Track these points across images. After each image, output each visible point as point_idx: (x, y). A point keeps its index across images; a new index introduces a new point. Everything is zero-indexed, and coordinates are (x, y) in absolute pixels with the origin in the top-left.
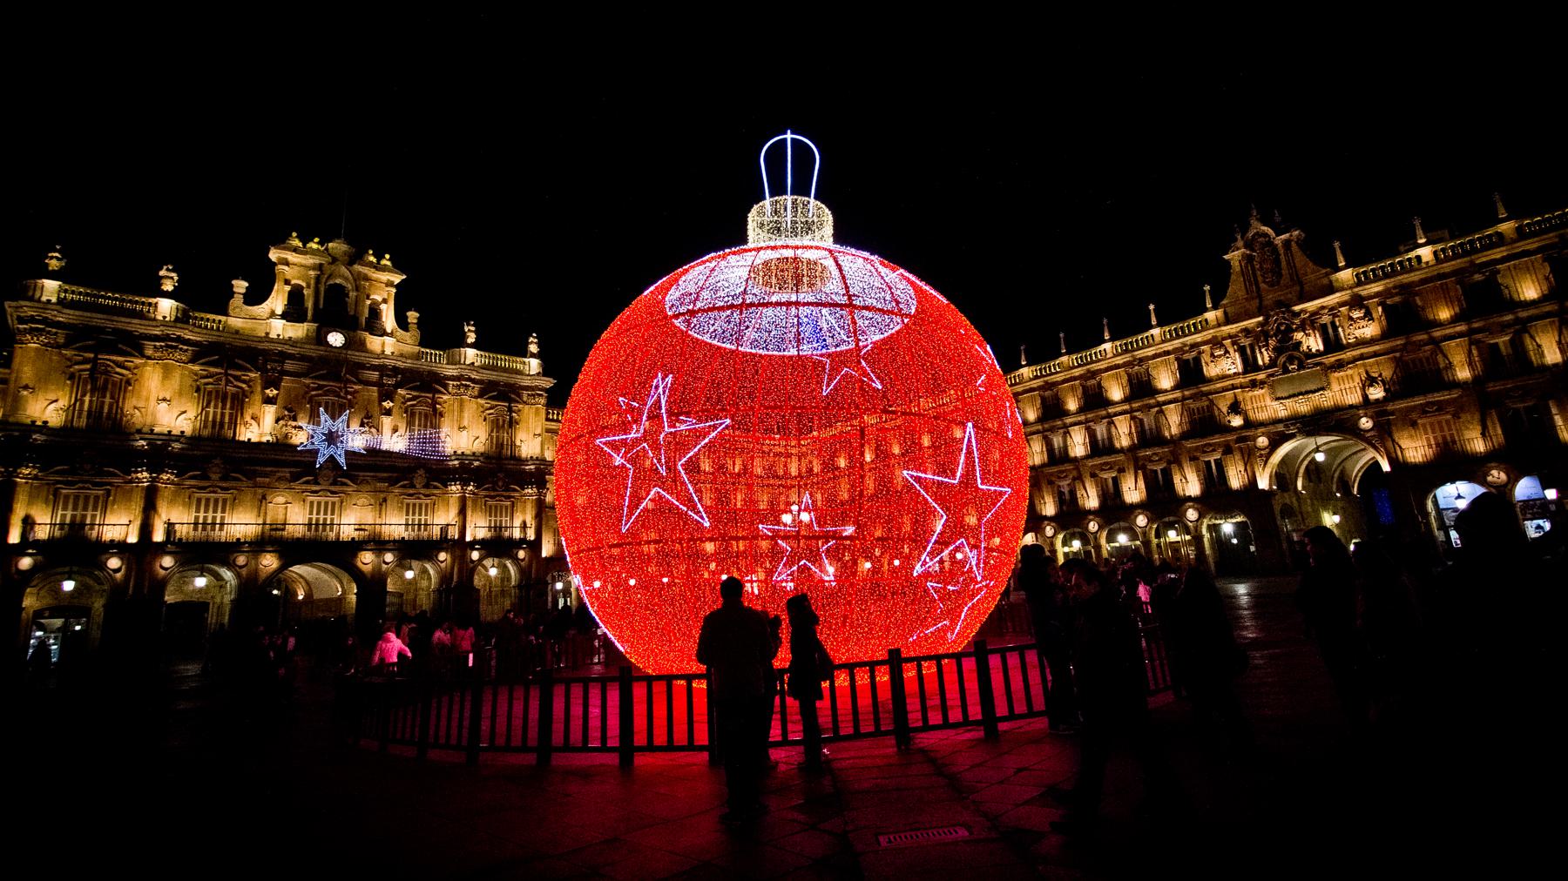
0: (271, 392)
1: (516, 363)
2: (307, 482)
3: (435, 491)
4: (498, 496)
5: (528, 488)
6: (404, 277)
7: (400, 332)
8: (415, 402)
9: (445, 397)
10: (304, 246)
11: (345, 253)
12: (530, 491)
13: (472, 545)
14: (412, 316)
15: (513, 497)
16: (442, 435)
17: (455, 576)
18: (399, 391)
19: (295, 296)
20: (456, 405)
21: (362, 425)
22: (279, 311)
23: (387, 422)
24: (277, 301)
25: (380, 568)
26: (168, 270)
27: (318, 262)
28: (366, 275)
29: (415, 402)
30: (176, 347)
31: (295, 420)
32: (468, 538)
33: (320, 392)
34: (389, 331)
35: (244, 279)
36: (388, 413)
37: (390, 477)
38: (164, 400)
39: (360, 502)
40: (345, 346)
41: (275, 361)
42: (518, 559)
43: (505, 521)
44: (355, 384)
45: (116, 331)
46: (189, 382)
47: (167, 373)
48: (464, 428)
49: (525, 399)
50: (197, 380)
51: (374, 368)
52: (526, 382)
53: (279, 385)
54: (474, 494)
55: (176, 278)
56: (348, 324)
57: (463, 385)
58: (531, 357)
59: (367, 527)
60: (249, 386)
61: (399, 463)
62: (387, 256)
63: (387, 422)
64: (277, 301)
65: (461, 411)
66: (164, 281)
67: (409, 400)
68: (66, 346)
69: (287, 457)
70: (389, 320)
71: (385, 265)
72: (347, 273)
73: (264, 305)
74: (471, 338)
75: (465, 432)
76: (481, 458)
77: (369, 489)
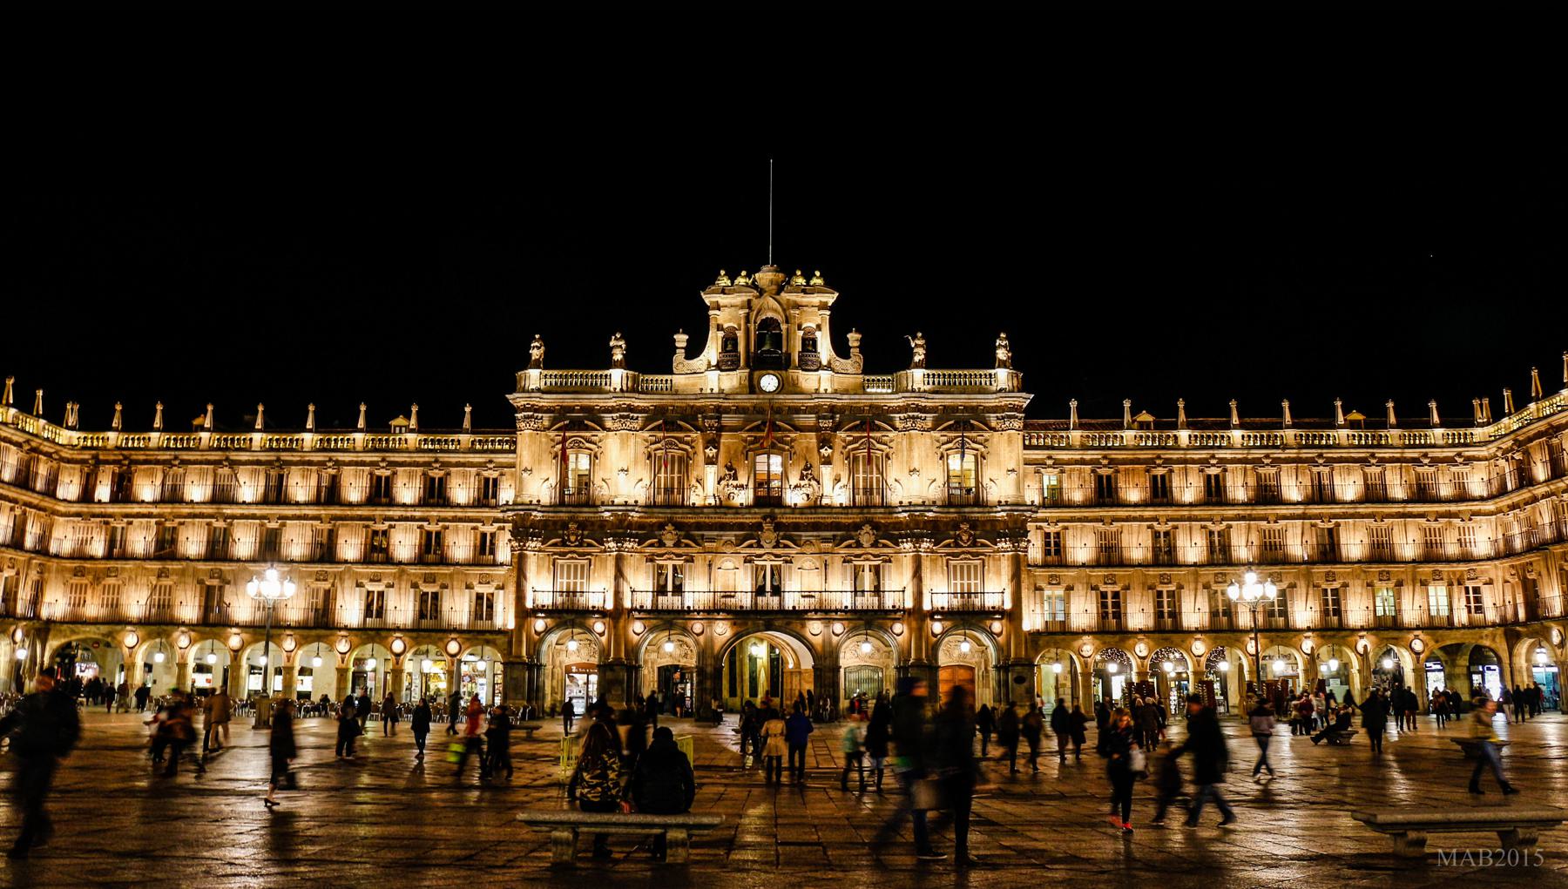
0: (711, 452)
1: (978, 375)
2: (750, 546)
3: (886, 550)
4: (963, 553)
5: (1001, 541)
6: (837, 294)
7: (840, 363)
8: (857, 445)
9: (892, 434)
10: (732, 283)
11: (772, 282)
12: (1003, 544)
13: (932, 614)
14: (853, 338)
15: (983, 554)
16: (890, 481)
17: (913, 656)
18: (841, 434)
19: (729, 341)
20: (904, 442)
21: (802, 478)
22: (714, 362)
23: (826, 473)
24: (712, 352)
25: (830, 643)
26: (616, 339)
27: (745, 299)
28: (795, 302)
29: (857, 445)
30: (628, 417)
31: (735, 478)
32: (927, 606)
33: (758, 445)
34: (825, 362)
35: (684, 333)
37: (834, 536)
39: (807, 565)
40: (781, 388)
41: (711, 418)
42: (992, 633)
43: (975, 584)
44: (789, 431)
45: (584, 409)
46: (641, 449)
47: (624, 443)
48: (915, 470)
49: (993, 424)
50: (647, 447)
52: (991, 401)
53: (719, 443)
54: (932, 552)
55: (624, 346)
56: (779, 363)
57: (909, 417)
58: (999, 367)
59: (813, 594)
60: (692, 447)
61: (844, 519)
62: (818, 273)
63: (826, 473)
64: (712, 352)
65: (910, 449)
66: (614, 351)
67: (851, 443)
68: (549, 429)
69: (729, 519)
70: (825, 349)
71: (814, 285)
72: (776, 305)
75: (915, 476)
76: (934, 509)
77: (814, 550)
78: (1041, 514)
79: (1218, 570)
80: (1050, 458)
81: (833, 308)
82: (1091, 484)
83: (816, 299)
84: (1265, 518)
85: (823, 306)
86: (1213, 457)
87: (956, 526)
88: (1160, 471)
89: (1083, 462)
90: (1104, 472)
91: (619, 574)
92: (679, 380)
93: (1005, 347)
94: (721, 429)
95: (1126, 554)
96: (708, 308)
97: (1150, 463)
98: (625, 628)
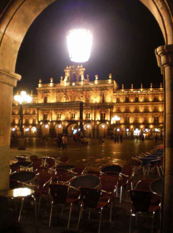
0: (65, 96)
7: (85, 80)
9: (92, 92)
14: (88, 76)
24: (66, 79)
31: (68, 100)
32: (96, 120)
36: (82, 96)
38: (52, 99)
42: (106, 124)
46: (55, 96)
49: (108, 89)
51: (80, 88)
56: (75, 81)
70: (83, 78)
73: (64, 80)
74: (97, 78)
75: (95, 99)
78: (116, 104)
79: (146, 113)
80: (118, 94)
81: (85, 71)
82: (125, 99)
83: (81, 70)
84: (155, 104)
85: (83, 71)
86: (146, 93)
87: (102, 106)
88: (137, 96)
89: (124, 95)
90: (127, 97)
91: (52, 115)
92: (61, 84)
93: (111, 76)
94: (66, 92)
95: (130, 111)
96: (65, 72)
97: (135, 95)
98: (53, 123)
